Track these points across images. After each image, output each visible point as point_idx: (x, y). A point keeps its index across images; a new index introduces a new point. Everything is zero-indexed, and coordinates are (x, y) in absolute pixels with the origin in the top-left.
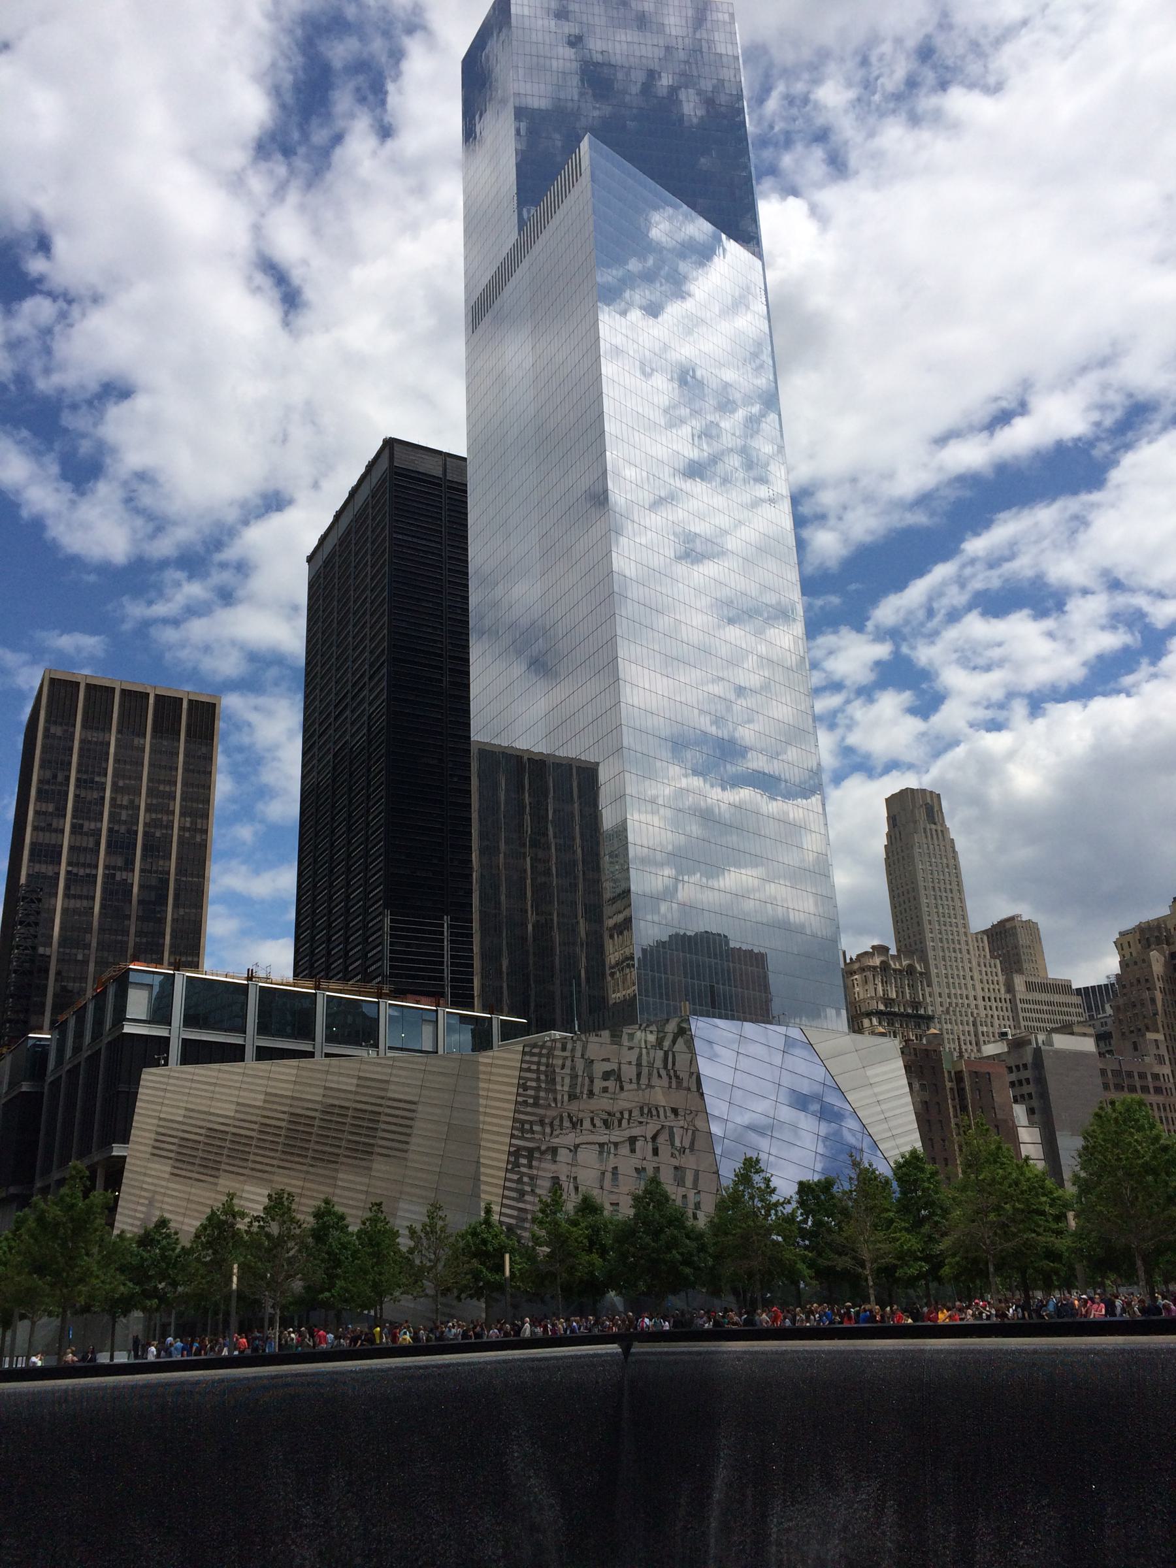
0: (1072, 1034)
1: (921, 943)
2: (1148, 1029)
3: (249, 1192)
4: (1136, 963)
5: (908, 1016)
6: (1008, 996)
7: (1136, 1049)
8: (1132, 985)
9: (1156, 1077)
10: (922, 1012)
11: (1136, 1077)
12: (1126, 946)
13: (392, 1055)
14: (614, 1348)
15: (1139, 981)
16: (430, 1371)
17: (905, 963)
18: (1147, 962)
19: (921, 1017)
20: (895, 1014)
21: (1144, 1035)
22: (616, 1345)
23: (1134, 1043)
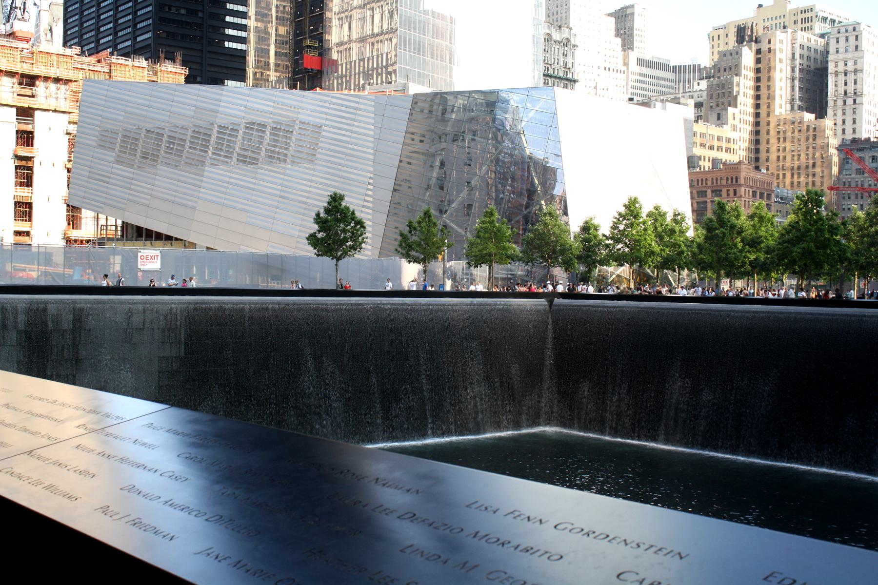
0: (679, 103)
1: (566, 19)
2: (730, 105)
3: (206, 182)
4: (731, 54)
5: (560, 78)
6: (625, 68)
7: (719, 119)
8: (725, 70)
9: (729, 140)
10: (570, 76)
11: (716, 139)
12: (716, 38)
13: (320, 91)
14: (543, 301)
15: (730, 69)
16: (405, 307)
17: (565, 36)
18: (738, 53)
19: (569, 80)
20: (550, 76)
21: (726, 109)
22: (543, 300)
23: (719, 115)
